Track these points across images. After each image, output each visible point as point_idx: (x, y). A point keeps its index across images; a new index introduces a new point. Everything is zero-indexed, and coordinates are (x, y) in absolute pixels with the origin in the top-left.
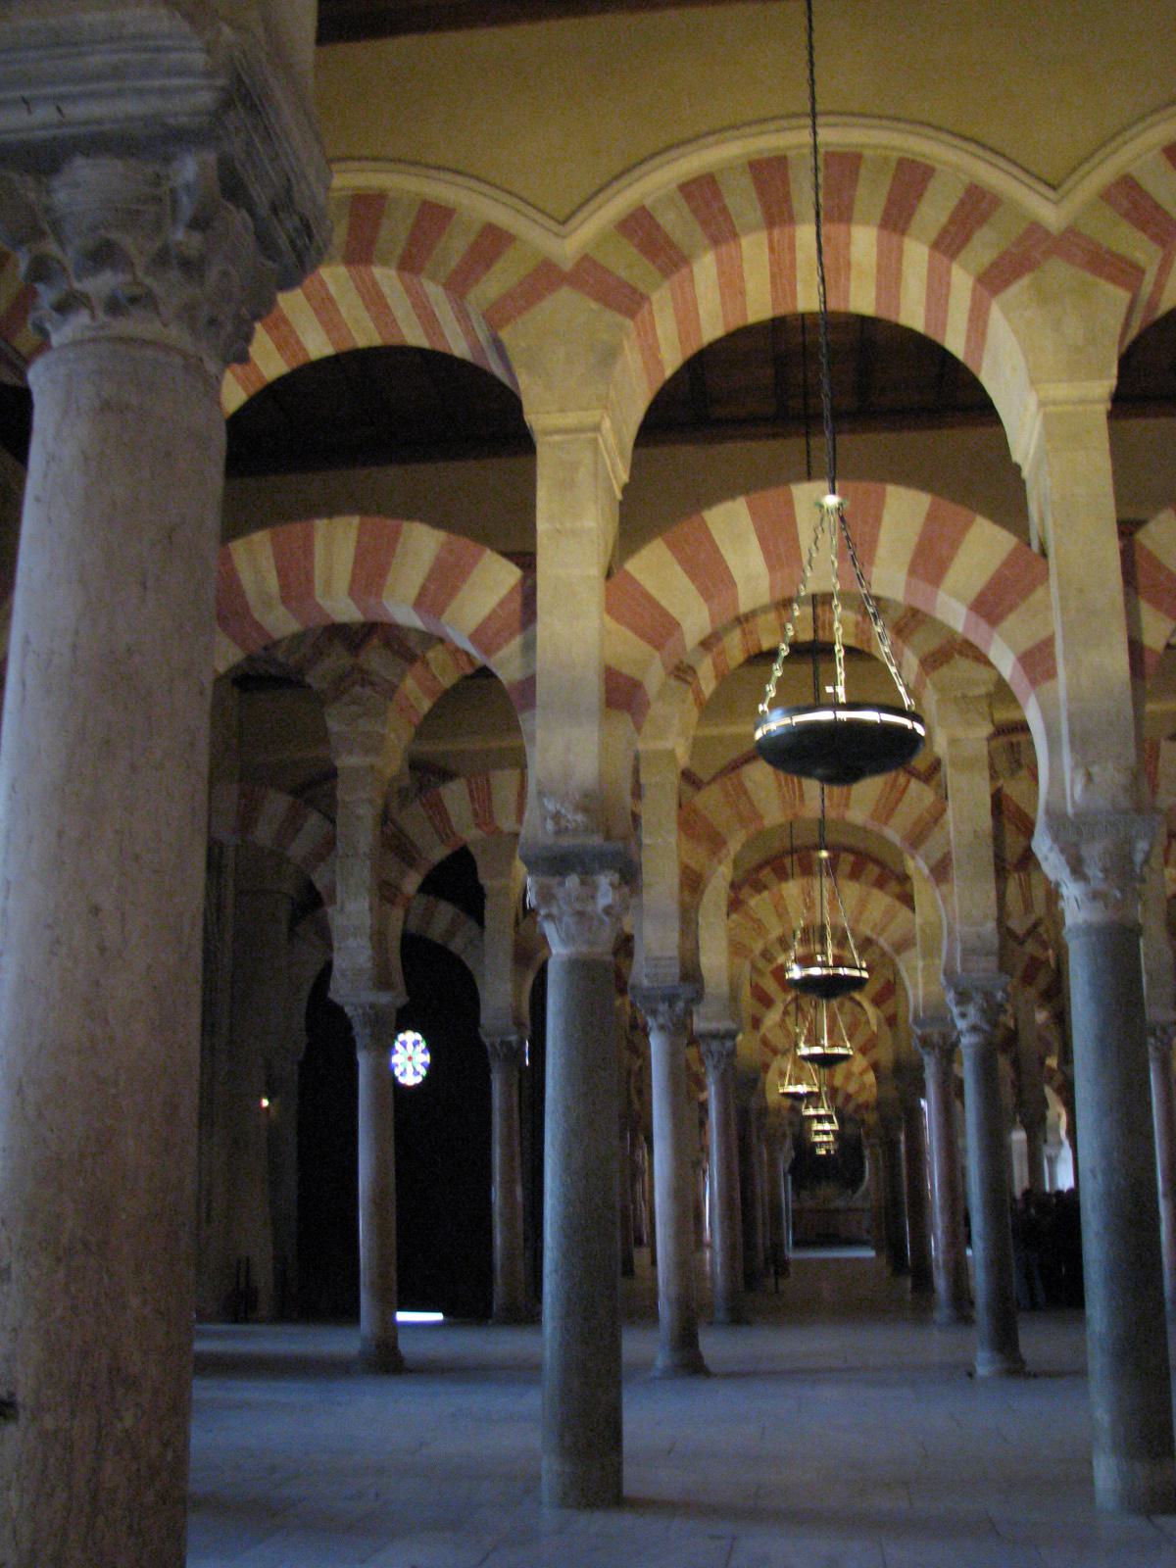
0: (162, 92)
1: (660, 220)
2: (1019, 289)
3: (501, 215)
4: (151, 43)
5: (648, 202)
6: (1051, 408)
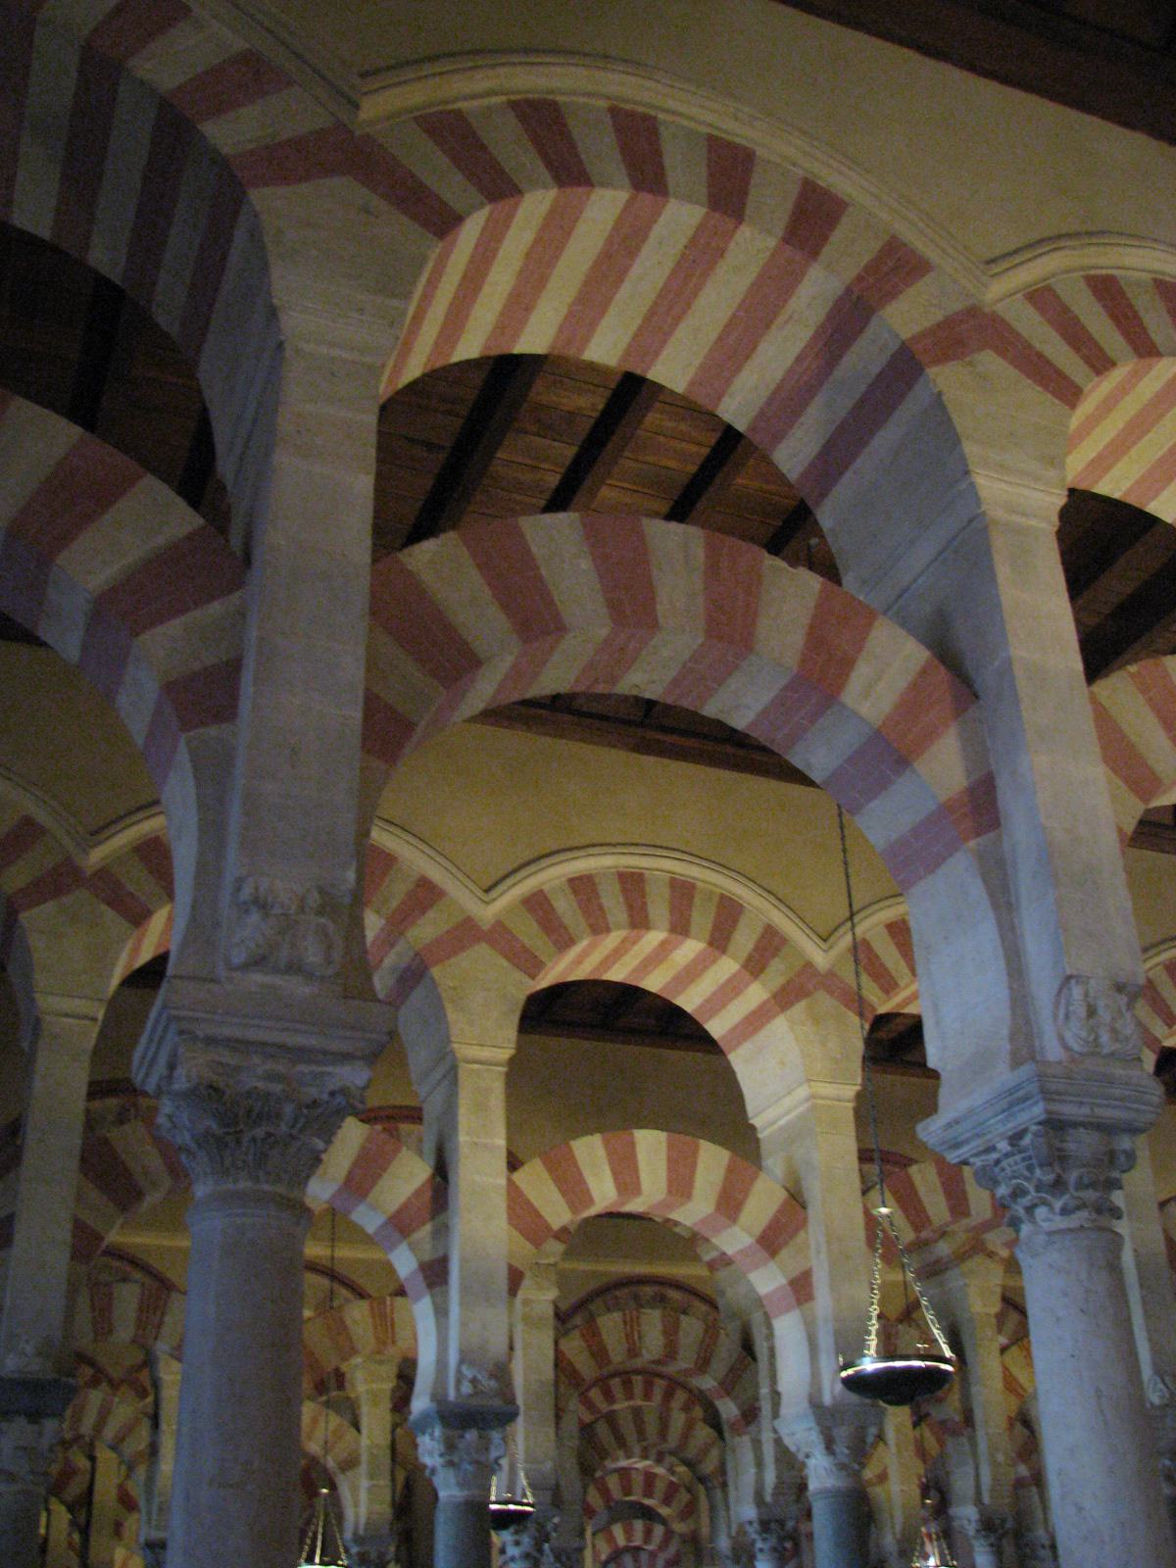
0: (1137, 1110)
1: (556, 904)
2: (800, 1008)
3: (436, 874)
4: (1141, 1089)
5: (543, 888)
6: (819, 1101)
